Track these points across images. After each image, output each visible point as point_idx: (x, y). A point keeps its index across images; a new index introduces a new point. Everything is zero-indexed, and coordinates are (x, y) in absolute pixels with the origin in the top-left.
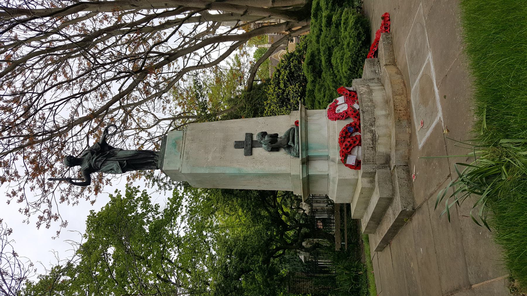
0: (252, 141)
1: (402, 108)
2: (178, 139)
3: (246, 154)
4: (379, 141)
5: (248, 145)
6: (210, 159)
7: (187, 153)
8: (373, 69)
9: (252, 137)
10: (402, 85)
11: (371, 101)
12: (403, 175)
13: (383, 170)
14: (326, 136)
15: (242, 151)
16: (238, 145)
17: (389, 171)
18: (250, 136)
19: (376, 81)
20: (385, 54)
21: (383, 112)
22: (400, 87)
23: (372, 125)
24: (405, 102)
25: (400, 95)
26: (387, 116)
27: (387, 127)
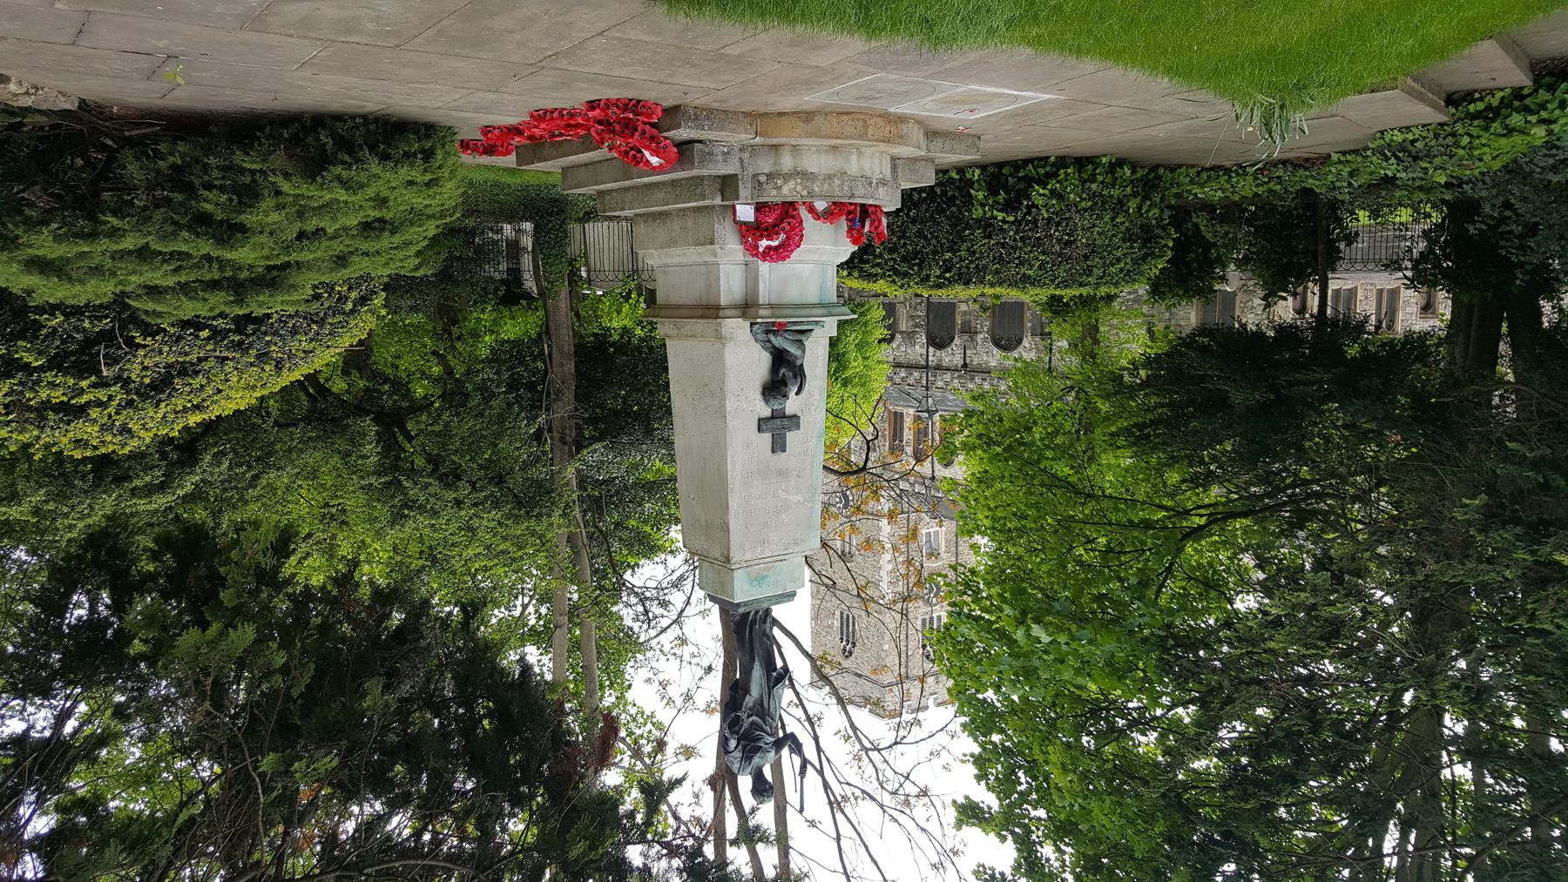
0: (772, 417)
5: (778, 426)
6: (799, 497)
7: (787, 546)
10: (845, 117)
11: (830, 177)
12: (938, 143)
16: (778, 445)
19: (746, 155)
20: (734, 131)
21: (854, 158)
24: (878, 120)
25: (866, 126)
26: (860, 153)
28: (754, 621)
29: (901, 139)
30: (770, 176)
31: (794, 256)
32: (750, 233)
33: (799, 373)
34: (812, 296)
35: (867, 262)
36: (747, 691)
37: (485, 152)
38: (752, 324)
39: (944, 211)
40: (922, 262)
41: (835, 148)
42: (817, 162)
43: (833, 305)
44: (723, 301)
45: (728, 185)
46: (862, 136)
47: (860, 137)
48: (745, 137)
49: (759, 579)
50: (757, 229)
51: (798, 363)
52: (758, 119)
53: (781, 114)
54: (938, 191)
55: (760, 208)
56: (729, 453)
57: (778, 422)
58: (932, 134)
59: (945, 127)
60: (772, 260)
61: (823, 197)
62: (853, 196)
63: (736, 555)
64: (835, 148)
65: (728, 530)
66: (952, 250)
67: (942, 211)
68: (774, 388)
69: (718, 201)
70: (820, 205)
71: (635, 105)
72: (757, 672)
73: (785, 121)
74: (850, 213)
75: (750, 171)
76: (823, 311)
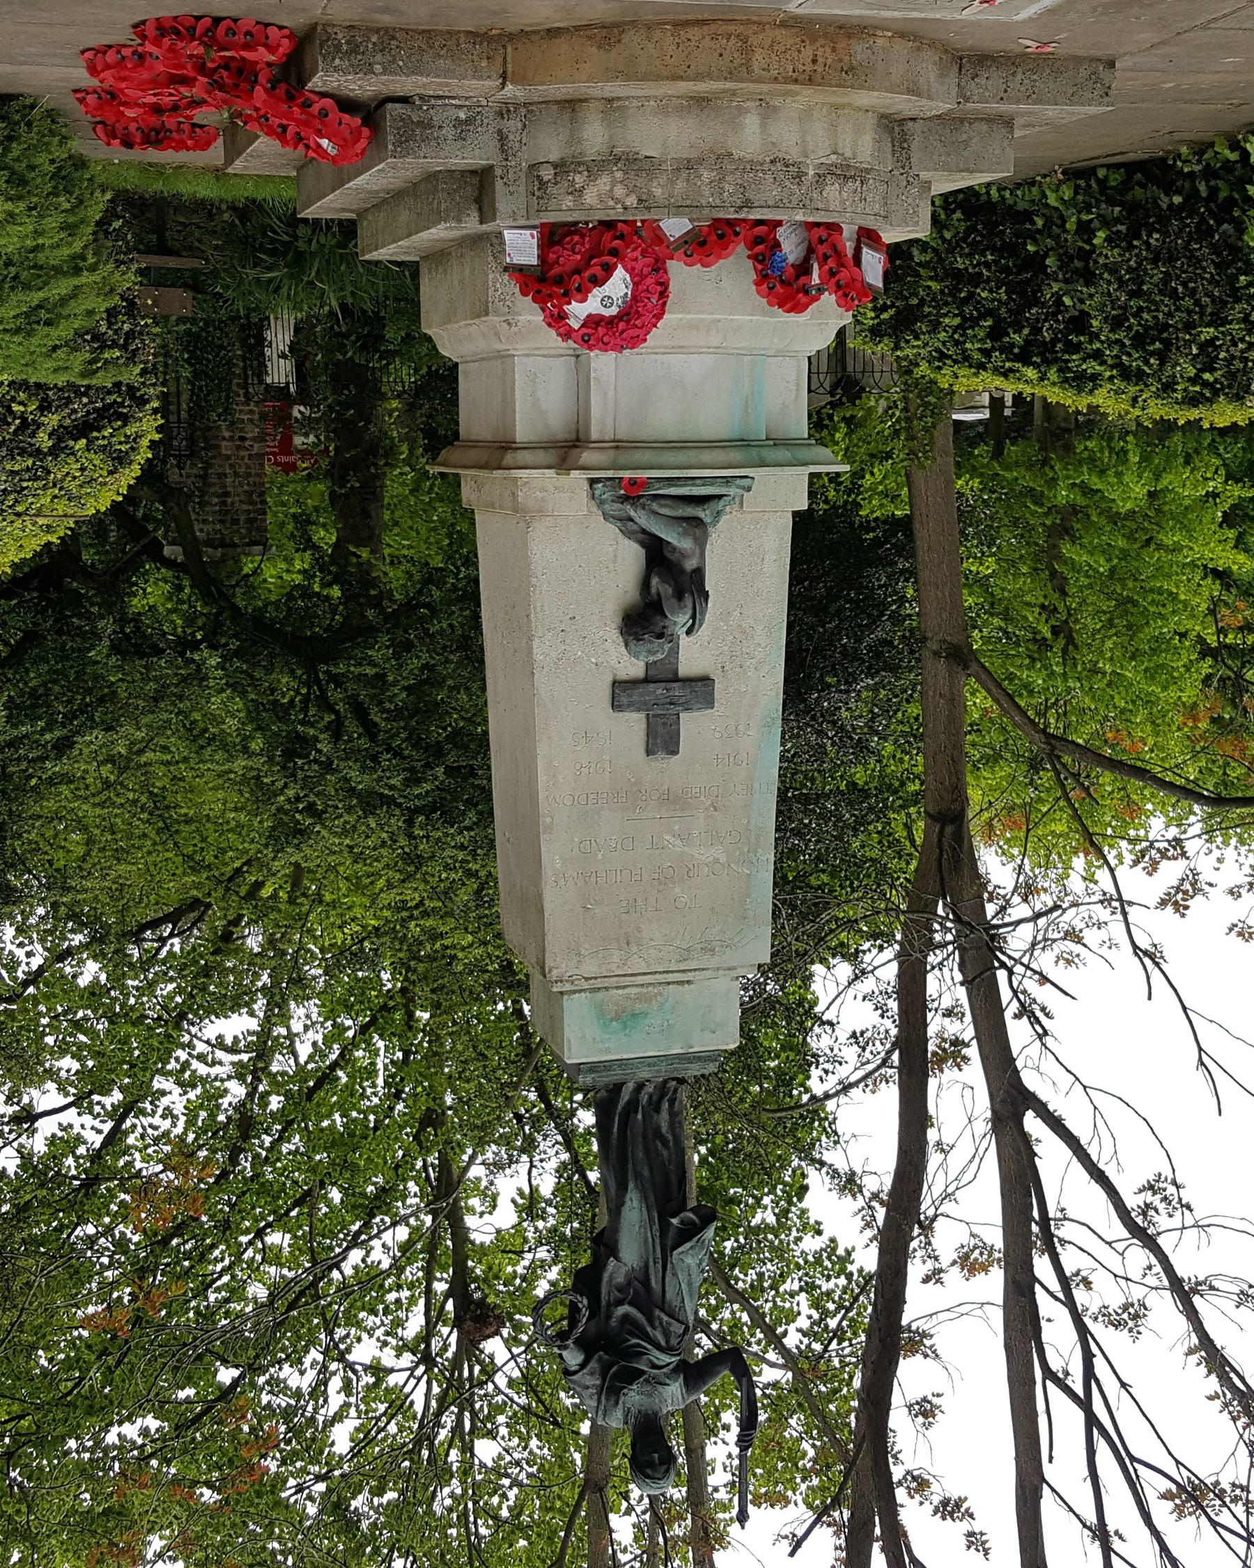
0: (647, 680)
1: (808, 53)
2: (601, 1012)
3: (709, 702)
4: (848, 154)
5: (662, 699)
8: (449, 132)
9: (634, 683)
10: (694, 33)
11: (689, 165)
12: (992, 80)
13: (914, 146)
14: (709, 359)
15: (691, 724)
16: (662, 739)
17: (918, 126)
18: (622, 693)
19: (513, 125)
20: (448, 73)
21: (751, 121)
22: (707, 42)
23: (800, 176)
24: (780, 34)
25: (747, 49)
26: (768, 111)
27: (806, 115)
28: (633, 1105)
29: (851, 74)
30: (561, 167)
31: (656, 337)
32: (549, 283)
33: (690, 586)
34: (714, 417)
35: (1077, 348)
36: (613, 1251)
37: (147, 141)
38: (593, 482)
39: (1210, 232)
40: (1167, 343)
41: (701, 102)
42: (660, 134)
43: (778, 442)
44: (522, 433)
45: (479, 188)
46: (741, 70)
47: (730, 75)
48: (476, 87)
49: (626, 1018)
50: (542, 279)
51: (690, 564)
52: (499, 45)
53: (553, 33)
54: (1203, 188)
55: (551, 237)
56: (542, 751)
57: (659, 690)
58: (970, 61)
59: (988, 43)
60: (605, 346)
61: (677, 209)
62: (748, 204)
63: (560, 965)
64: (701, 102)
65: (541, 911)
66: (1218, 320)
67: (1204, 232)
68: (642, 621)
69: (471, 225)
70: (675, 227)
71: (212, 29)
72: (634, 1212)
73: (562, 46)
74: (758, 240)
75: (525, 158)
76: (735, 456)
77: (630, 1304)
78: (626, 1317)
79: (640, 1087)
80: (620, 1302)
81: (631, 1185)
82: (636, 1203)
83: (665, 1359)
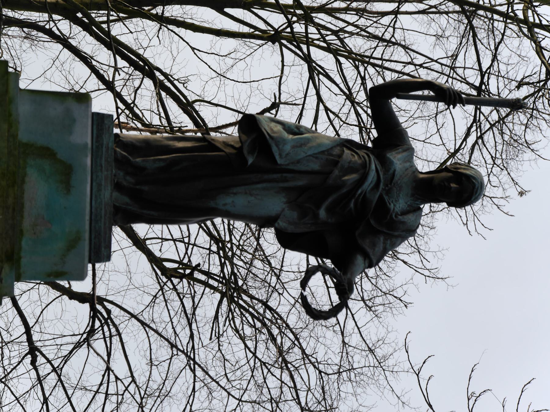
77: (319, 207)
78: (329, 210)
79: (118, 187)
80: (316, 216)
81: (212, 204)
82: (229, 200)
83: (372, 176)
